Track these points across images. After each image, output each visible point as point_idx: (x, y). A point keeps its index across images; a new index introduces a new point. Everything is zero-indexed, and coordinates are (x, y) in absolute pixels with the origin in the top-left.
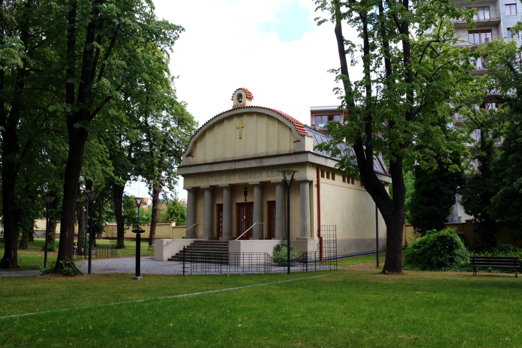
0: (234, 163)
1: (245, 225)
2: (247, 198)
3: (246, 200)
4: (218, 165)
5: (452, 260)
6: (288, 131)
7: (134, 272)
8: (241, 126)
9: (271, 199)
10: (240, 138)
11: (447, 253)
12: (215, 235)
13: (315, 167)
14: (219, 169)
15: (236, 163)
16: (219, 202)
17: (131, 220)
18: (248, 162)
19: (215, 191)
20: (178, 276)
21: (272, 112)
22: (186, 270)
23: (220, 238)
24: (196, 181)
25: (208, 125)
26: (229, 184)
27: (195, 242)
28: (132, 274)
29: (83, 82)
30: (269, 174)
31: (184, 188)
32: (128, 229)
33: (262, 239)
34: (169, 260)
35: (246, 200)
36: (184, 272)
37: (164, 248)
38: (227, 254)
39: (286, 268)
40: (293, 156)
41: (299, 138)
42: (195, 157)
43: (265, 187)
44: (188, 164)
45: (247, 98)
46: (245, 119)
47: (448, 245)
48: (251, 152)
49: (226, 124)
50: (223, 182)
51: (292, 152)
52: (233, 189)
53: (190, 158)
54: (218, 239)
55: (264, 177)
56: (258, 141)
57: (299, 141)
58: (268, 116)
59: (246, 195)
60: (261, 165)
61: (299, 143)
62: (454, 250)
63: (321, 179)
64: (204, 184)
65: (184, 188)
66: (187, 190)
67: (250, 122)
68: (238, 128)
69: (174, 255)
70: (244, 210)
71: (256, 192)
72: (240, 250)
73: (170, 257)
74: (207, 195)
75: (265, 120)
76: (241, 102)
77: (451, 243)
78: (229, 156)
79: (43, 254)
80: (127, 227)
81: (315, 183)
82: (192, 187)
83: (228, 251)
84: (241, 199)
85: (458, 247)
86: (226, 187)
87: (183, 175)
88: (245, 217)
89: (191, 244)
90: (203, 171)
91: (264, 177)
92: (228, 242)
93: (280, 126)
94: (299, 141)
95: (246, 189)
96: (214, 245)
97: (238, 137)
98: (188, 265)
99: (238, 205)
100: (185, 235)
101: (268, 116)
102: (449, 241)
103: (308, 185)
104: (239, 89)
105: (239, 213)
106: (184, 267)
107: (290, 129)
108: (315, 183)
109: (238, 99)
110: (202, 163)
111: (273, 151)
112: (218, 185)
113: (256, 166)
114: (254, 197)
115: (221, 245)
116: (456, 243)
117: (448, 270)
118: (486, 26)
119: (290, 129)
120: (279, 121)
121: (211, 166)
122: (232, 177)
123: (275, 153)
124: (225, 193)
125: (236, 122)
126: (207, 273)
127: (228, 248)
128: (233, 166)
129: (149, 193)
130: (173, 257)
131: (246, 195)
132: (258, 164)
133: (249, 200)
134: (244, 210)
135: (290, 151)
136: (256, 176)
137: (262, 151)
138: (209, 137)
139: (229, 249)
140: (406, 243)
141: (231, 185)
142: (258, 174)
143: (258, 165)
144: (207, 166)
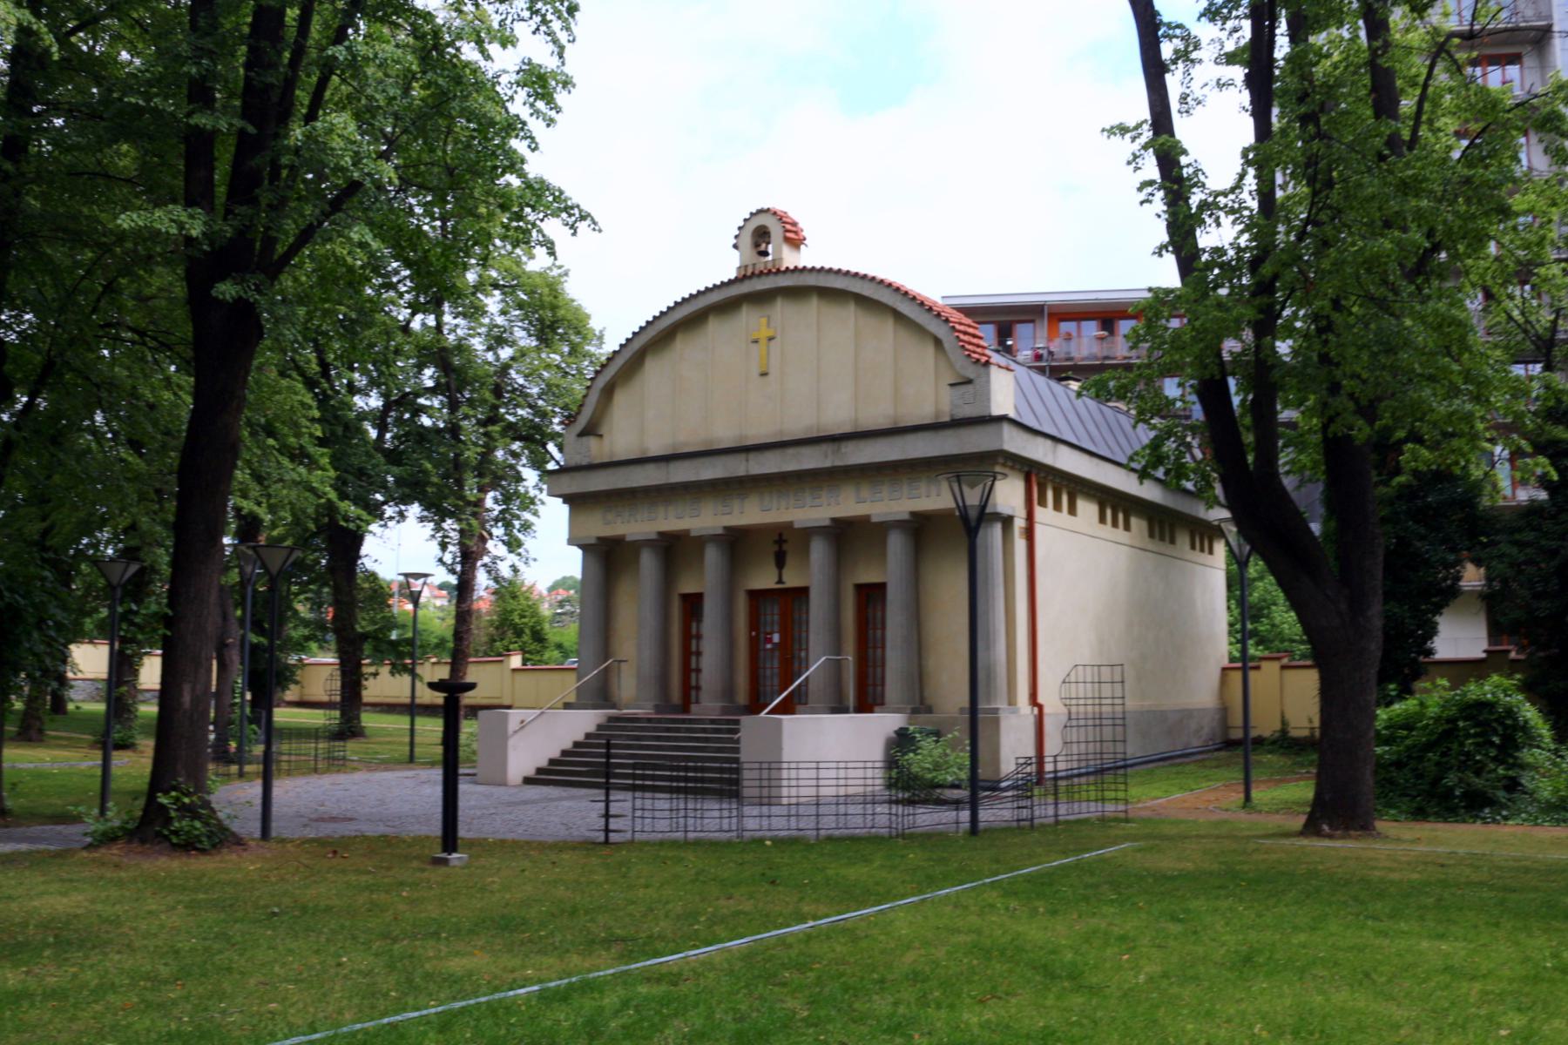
0: (743, 456)
1: (776, 664)
3: (780, 581)
5: (1513, 785)
6: (929, 350)
7: (436, 828)
8: (764, 333)
9: (869, 576)
10: (764, 374)
11: (1494, 759)
12: (676, 695)
13: (1020, 470)
14: (693, 478)
15: (752, 456)
16: (688, 586)
17: (384, 647)
18: (791, 451)
19: (674, 549)
20: (587, 845)
21: (873, 285)
22: (613, 824)
23: (693, 707)
24: (610, 516)
25: (652, 332)
26: (726, 528)
27: (611, 719)
28: (419, 840)
29: (251, 129)
30: (865, 492)
31: (571, 542)
32: (375, 675)
33: (846, 711)
34: (528, 781)
35: (780, 581)
36: (607, 830)
37: (511, 742)
38: (737, 760)
39: (965, 815)
40: (949, 432)
41: (970, 372)
42: (606, 439)
43: (847, 536)
45: (787, 240)
47: (1495, 732)
48: (798, 423)
49: (715, 328)
50: (706, 519)
51: (947, 419)
52: (736, 542)
53: (592, 442)
54: (686, 710)
55: (848, 504)
56: (822, 382)
57: (969, 382)
58: (862, 301)
59: (780, 562)
60: (838, 463)
61: (970, 387)
62: (1518, 748)
63: (1039, 512)
64: (639, 525)
65: (571, 542)
66: (580, 546)
67: (797, 323)
68: (756, 342)
69: (543, 763)
70: (772, 615)
71: (819, 551)
72: (779, 748)
73: (531, 772)
74: (648, 563)
75: (849, 314)
76: (765, 254)
77: (1506, 727)
78: (725, 434)
80: (372, 669)
81: (1019, 523)
82: (599, 539)
83: (737, 750)
84: (764, 579)
85: (1532, 740)
86: (714, 538)
87: (568, 499)
88: (776, 638)
89: (600, 727)
92: (737, 722)
93: (905, 336)
94: (969, 382)
95: (783, 543)
96: (678, 730)
97: (755, 371)
98: (622, 802)
99: (756, 596)
100: (572, 699)
101: (862, 301)
102: (1500, 721)
103: (997, 529)
104: (760, 211)
105: (755, 623)
106: (607, 816)
107: (938, 342)
108: (1019, 523)
109: (757, 245)
111: (877, 415)
112: (687, 532)
114: (812, 570)
115: (704, 731)
116: (1525, 728)
117: (1506, 818)
118: (1504, 43)
119: (938, 342)
120: (898, 316)
121: (663, 465)
123: (883, 423)
124: (712, 556)
125: (749, 320)
126: (691, 835)
127: (738, 741)
129: (440, 560)
130: (539, 771)
131: (780, 562)
132: (831, 458)
133: (792, 580)
134: (772, 615)
135: (937, 414)
136: (817, 501)
137: (838, 414)
138: (655, 371)
139: (743, 746)
140: (1284, 722)
141: (730, 530)
143: (828, 464)
144: (650, 468)
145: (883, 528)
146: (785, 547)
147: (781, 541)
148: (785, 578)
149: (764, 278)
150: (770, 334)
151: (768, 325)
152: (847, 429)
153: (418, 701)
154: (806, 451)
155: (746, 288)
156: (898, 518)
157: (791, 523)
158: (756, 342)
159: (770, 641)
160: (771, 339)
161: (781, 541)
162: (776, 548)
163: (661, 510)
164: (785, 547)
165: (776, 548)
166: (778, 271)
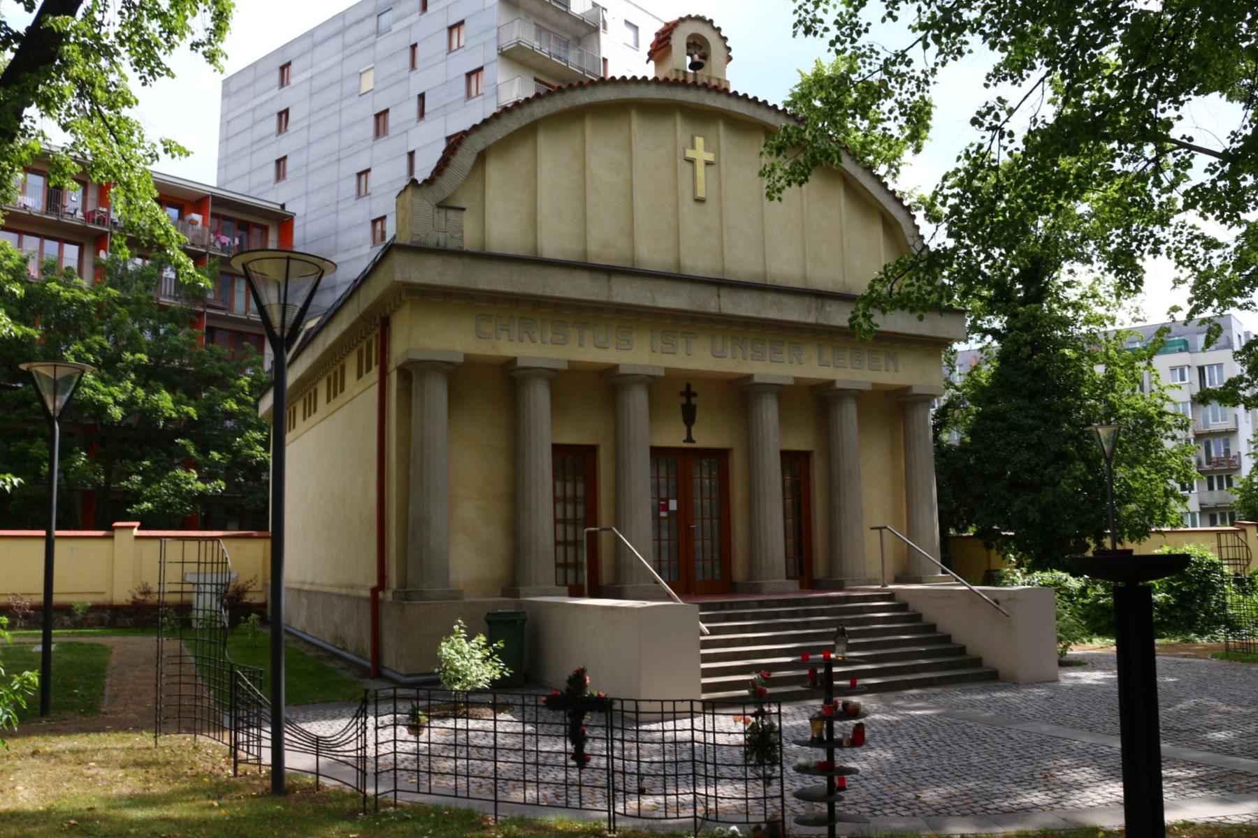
0: (714, 290)
2: (694, 429)
3: (689, 439)
4: (637, 283)
14: (647, 303)
15: (723, 291)
18: (771, 297)
30: (828, 355)
35: (689, 439)
43: (820, 400)
44: (453, 245)
50: (639, 355)
59: (689, 416)
60: (822, 321)
78: (651, 254)
88: (673, 505)
90: (558, 294)
97: (688, 197)
104: (700, 19)
110: (510, 251)
113: (803, 319)
121: (603, 279)
122: (681, 343)
128: (710, 302)
131: (689, 416)
133: (705, 438)
142: (785, 349)
143: (811, 319)
145: (846, 393)
146: (694, 401)
147: (688, 393)
148: (694, 437)
150: (710, 157)
151: (706, 150)
152: (830, 287)
153: (57, 599)
154: (789, 301)
155: (690, 97)
156: (862, 387)
157: (750, 376)
158: (692, 161)
159: (666, 508)
160: (708, 164)
161: (688, 393)
162: (684, 400)
163: (574, 333)
164: (694, 401)
165: (684, 400)
166: (726, 90)
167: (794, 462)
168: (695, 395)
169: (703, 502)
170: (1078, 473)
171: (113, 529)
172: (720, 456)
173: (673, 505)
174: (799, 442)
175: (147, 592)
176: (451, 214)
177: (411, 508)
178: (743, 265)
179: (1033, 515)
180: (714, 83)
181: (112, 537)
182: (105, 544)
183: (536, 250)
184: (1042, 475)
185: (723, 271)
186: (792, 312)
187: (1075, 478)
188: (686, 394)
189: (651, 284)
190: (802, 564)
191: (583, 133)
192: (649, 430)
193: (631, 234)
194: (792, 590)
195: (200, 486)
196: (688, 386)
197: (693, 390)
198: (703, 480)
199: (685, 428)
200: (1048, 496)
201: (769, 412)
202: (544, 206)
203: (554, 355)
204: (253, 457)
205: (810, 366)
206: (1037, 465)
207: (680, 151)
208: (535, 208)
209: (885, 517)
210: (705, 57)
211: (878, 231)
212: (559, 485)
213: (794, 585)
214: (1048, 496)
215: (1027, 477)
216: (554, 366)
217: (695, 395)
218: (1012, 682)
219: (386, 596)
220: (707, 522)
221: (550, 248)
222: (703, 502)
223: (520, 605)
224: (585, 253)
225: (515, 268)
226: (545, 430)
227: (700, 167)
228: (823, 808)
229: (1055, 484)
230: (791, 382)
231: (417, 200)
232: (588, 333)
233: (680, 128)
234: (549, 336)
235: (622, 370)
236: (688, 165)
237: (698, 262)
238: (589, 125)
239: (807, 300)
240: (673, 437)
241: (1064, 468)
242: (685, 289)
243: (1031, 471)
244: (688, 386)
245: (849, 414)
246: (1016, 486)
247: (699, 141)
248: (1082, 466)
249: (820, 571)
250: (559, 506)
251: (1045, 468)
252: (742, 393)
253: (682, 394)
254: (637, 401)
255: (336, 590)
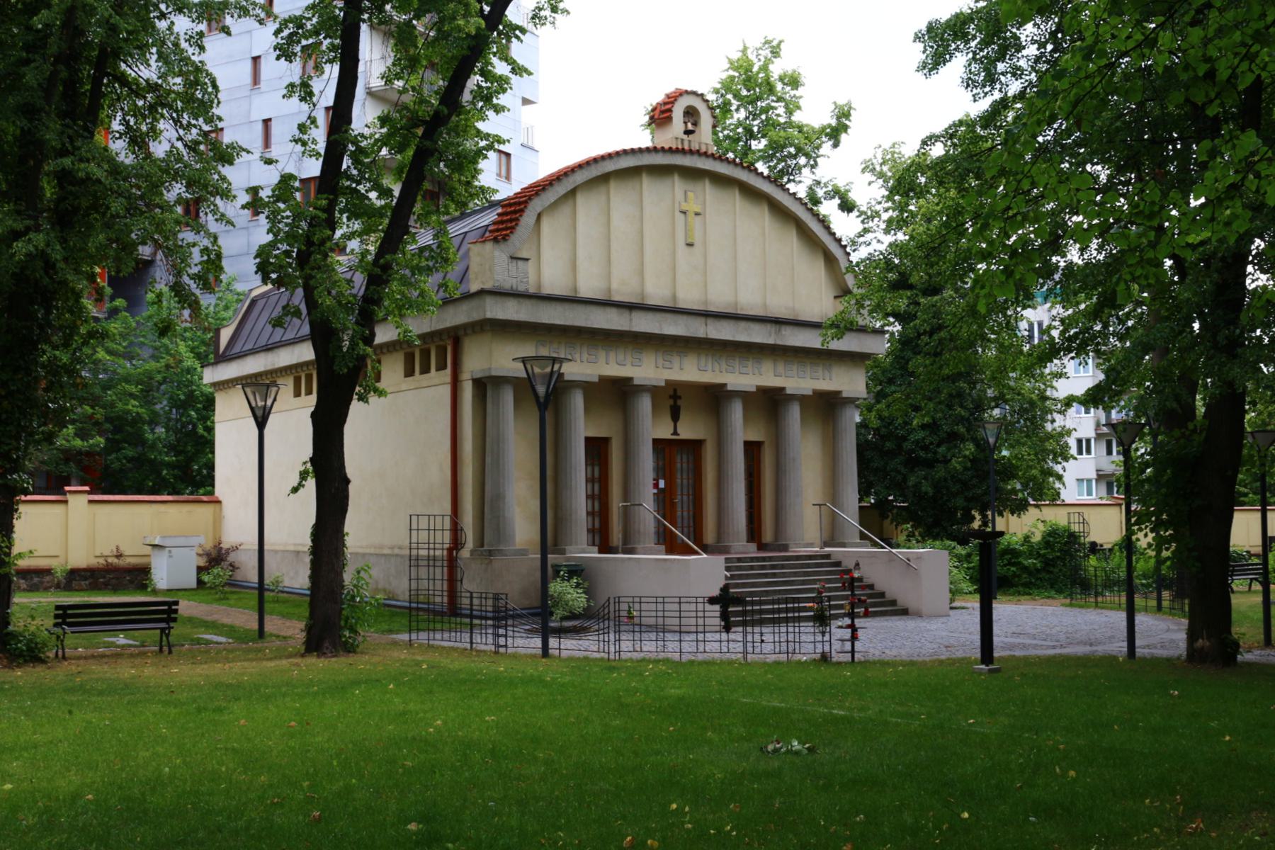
0: (702, 320)
3: (675, 433)
14: (657, 331)
15: (710, 321)
18: (743, 324)
30: (781, 367)
35: (675, 433)
46: (707, 188)
50: (648, 370)
59: (675, 417)
79: (537, 642)
91: (767, 376)
104: (694, 93)
121: (626, 313)
122: (676, 360)
131: (675, 417)
133: (687, 431)
136: (744, 370)
142: (750, 363)
143: (771, 341)
146: (679, 402)
148: (679, 431)
149: (703, 158)
150: (698, 210)
157: (725, 385)
158: (684, 213)
160: (697, 214)
162: (671, 402)
163: (602, 354)
165: (671, 402)
167: (752, 449)
168: (680, 398)
169: (682, 480)
170: (967, 453)
171: (64, 493)
172: (695, 446)
173: (662, 484)
174: (753, 436)
175: (119, 556)
176: (520, 263)
177: (488, 487)
178: (719, 298)
179: (927, 488)
180: (703, 150)
181: (66, 502)
182: (58, 509)
183: (575, 290)
184: (935, 453)
185: (706, 302)
186: (758, 335)
187: (965, 456)
188: (673, 398)
189: (659, 316)
190: (754, 532)
191: (608, 193)
192: (652, 426)
193: (641, 273)
194: (752, 550)
195: (78, 443)
196: (675, 391)
197: (679, 393)
198: (681, 462)
199: (672, 424)
200: (940, 472)
201: (736, 412)
202: (581, 253)
203: (589, 371)
204: (129, 412)
205: (767, 376)
206: (932, 443)
207: (677, 205)
208: (575, 254)
209: (817, 494)
210: (695, 124)
211: (819, 266)
212: (589, 469)
213: (753, 546)
214: (940, 472)
215: (922, 454)
216: (588, 379)
217: (680, 398)
218: (919, 615)
219: (465, 553)
220: (685, 498)
221: (588, 288)
222: (682, 480)
223: (569, 559)
224: (609, 290)
225: (567, 306)
226: (581, 425)
227: (691, 215)
228: (848, 646)
229: (946, 461)
230: (754, 389)
231: (497, 253)
232: (612, 355)
233: (678, 185)
234: (585, 356)
235: (636, 382)
236: (682, 216)
237: (689, 297)
238: (613, 184)
239: (769, 326)
240: (665, 432)
241: (955, 446)
242: (683, 320)
243: (925, 448)
244: (675, 391)
245: (794, 414)
246: (913, 463)
247: (690, 195)
248: (971, 447)
249: (768, 537)
250: (590, 486)
251: (939, 445)
252: (714, 398)
253: (671, 397)
254: (645, 405)
255: (372, 551)
